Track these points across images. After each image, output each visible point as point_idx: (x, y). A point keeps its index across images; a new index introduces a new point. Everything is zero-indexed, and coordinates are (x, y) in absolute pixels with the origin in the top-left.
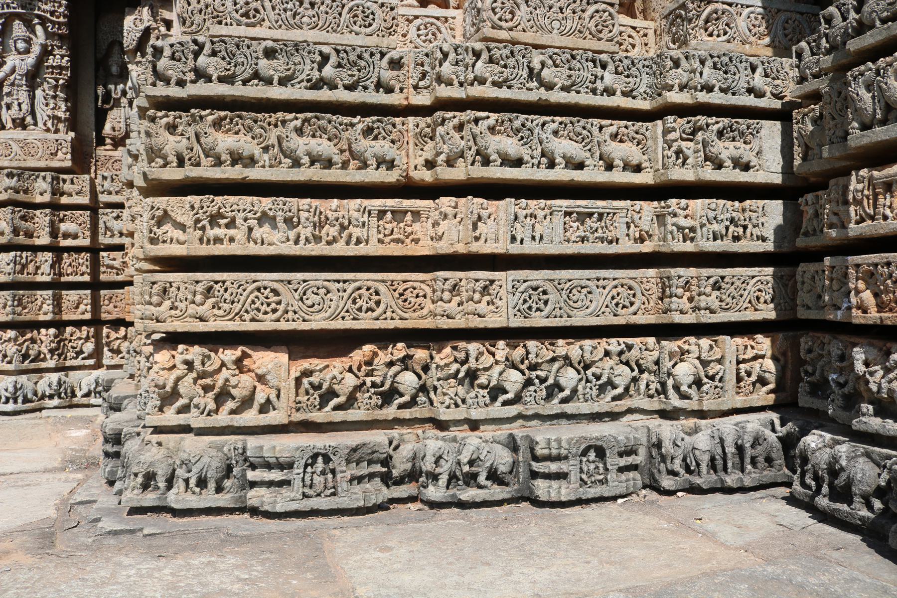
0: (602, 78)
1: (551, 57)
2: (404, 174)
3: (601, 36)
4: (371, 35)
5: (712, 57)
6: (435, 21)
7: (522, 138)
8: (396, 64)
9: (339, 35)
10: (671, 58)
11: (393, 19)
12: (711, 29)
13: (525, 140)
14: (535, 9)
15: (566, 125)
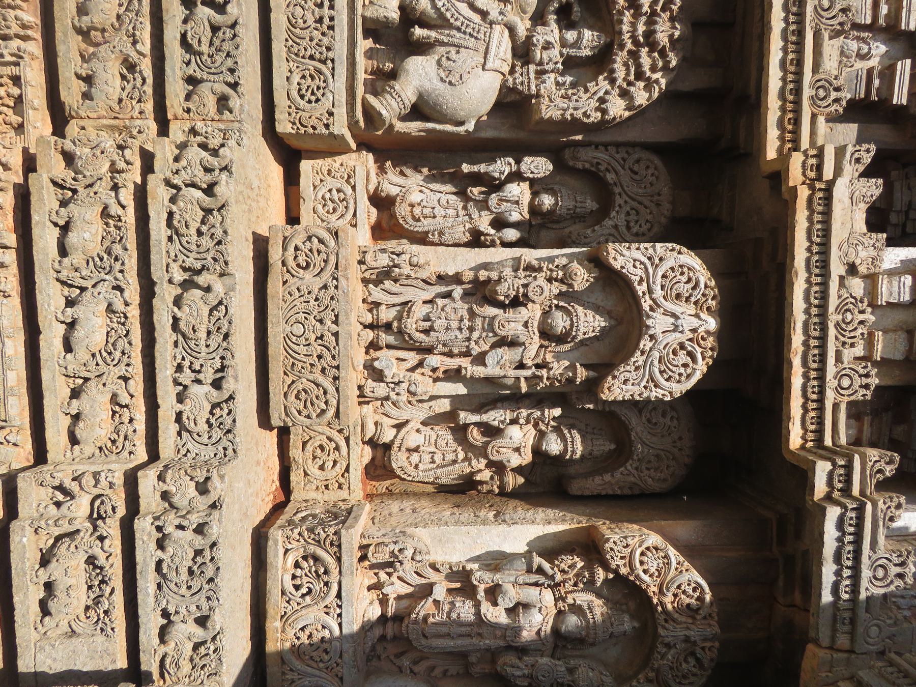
0: (198, 381)
1: (220, 303)
2: (73, 113)
3: (292, 398)
4: (289, 99)
5: (214, 545)
6: (351, 212)
7: (101, 259)
8: (223, 102)
9: (285, 55)
10: (207, 479)
11: (314, 128)
12: (305, 564)
13: (99, 263)
14: (317, 299)
15: (123, 324)
